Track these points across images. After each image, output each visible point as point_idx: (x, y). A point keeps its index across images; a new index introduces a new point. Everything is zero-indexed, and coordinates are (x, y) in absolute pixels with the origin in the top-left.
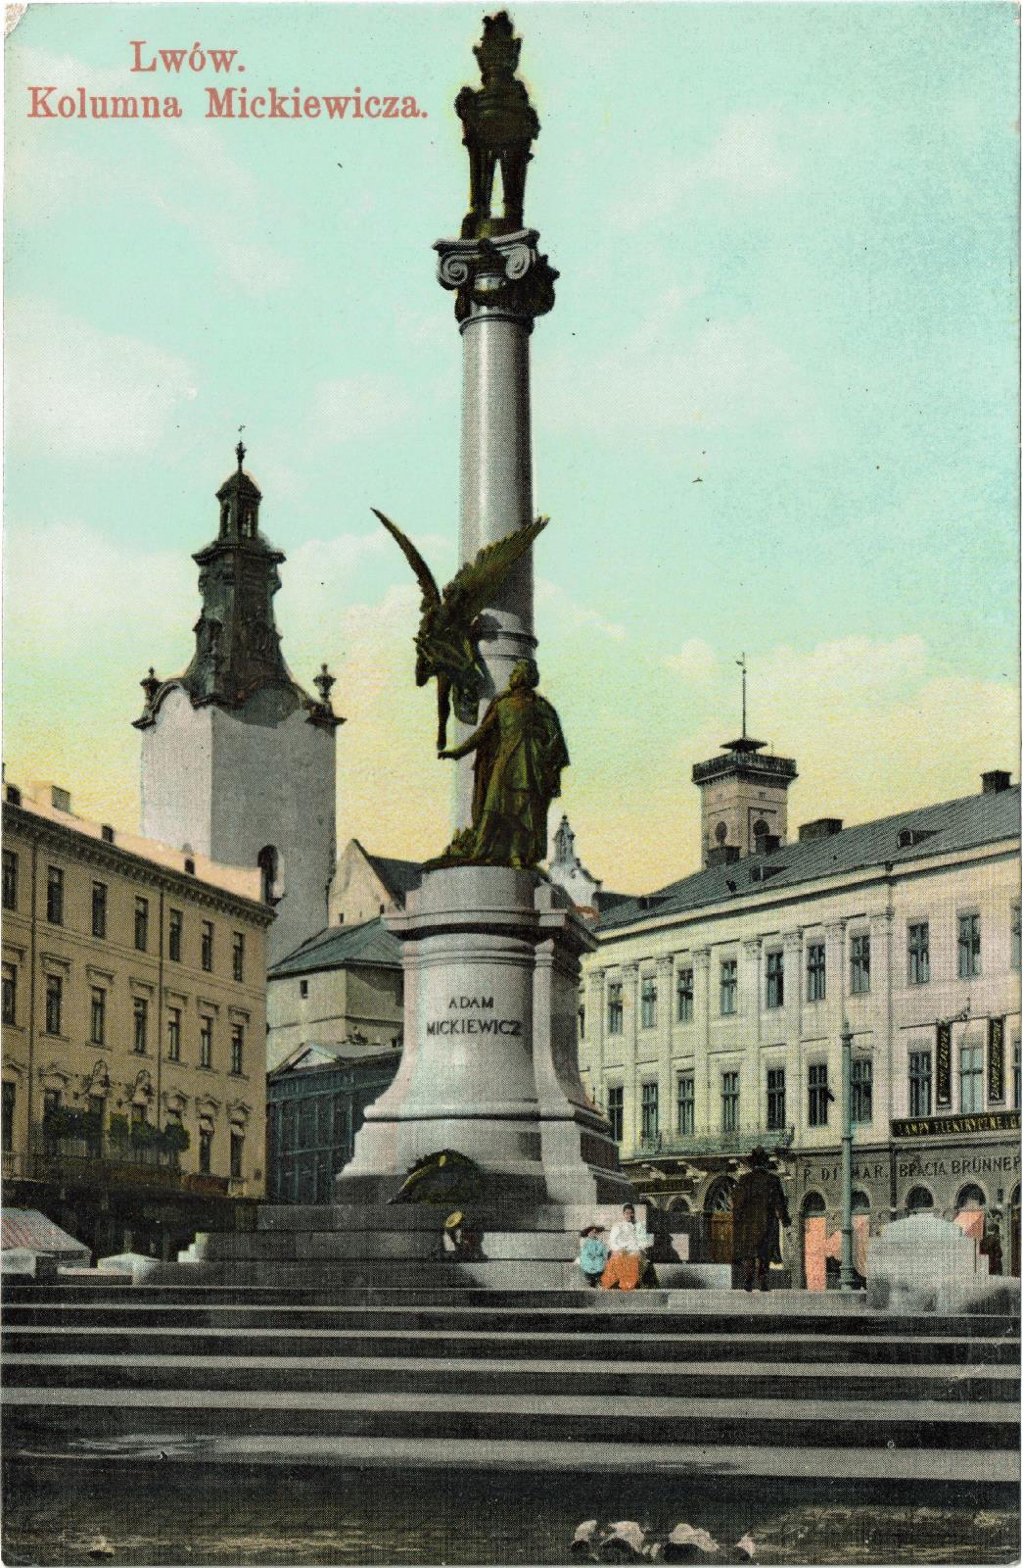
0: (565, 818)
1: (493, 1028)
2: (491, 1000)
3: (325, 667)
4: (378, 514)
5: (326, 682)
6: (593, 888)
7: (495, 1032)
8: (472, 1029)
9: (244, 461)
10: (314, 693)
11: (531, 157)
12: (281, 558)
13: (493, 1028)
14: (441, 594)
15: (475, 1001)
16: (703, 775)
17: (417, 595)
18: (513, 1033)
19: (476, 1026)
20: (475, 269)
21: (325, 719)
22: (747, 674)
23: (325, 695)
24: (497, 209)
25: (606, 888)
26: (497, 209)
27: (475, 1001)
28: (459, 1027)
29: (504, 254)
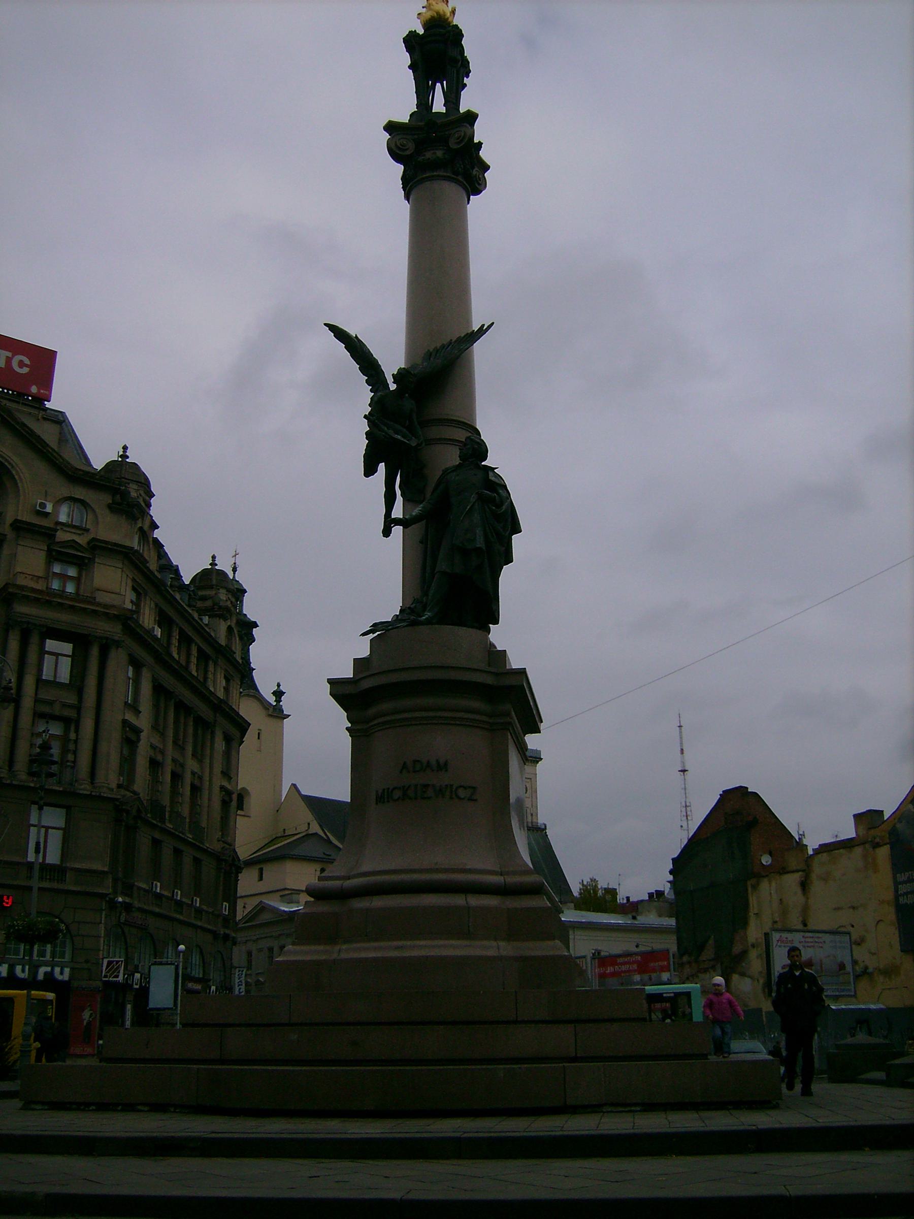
2: (446, 764)
3: (279, 685)
4: (333, 328)
5: (279, 694)
7: (451, 798)
9: (236, 573)
10: (272, 700)
12: (255, 625)
14: (390, 380)
15: (428, 762)
17: (365, 394)
18: (470, 799)
20: (421, 145)
21: (277, 713)
23: (278, 700)
24: (439, 105)
26: (439, 105)
27: (428, 764)
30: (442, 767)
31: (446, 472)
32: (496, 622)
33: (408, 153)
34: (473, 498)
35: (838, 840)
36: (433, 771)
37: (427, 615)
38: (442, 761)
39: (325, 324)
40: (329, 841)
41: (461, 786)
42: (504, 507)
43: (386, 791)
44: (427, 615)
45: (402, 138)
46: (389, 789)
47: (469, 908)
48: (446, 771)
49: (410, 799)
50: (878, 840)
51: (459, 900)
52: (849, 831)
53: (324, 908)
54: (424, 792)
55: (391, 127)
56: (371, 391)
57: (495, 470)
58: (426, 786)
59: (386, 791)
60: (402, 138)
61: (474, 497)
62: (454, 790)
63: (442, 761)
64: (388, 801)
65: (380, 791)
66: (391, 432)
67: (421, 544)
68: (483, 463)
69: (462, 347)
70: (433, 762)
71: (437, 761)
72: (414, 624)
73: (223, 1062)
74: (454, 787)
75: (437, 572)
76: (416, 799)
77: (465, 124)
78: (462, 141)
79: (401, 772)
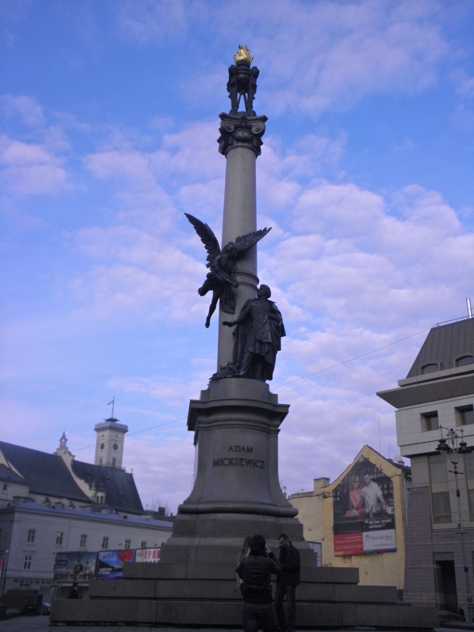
0: (64, 433)
1: (252, 464)
2: (252, 449)
6: (71, 458)
7: (254, 466)
8: (242, 464)
11: (254, 98)
13: (252, 464)
16: (98, 429)
17: (205, 253)
18: (262, 467)
19: (244, 462)
22: (114, 399)
25: (76, 459)
27: (243, 448)
28: (234, 462)
29: (251, 124)
30: (250, 450)
31: (249, 302)
32: (270, 378)
33: (231, 131)
34: (266, 317)
35: (304, 492)
36: (245, 451)
37: (242, 373)
38: (250, 448)
39: (185, 214)
40: (10, 469)
41: (258, 461)
42: (280, 324)
43: (220, 461)
44: (242, 373)
45: (229, 123)
46: (221, 459)
47: (266, 523)
48: (252, 452)
49: (234, 465)
50: (326, 494)
51: (260, 518)
52: (310, 487)
53: (186, 517)
54: (241, 462)
55: (223, 116)
56: (208, 252)
57: (275, 304)
58: (242, 459)
59: (220, 461)
60: (228, 123)
61: (267, 316)
62: (255, 463)
63: (250, 448)
64: (221, 465)
65: (216, 460)
66: (224, 277)
67: (232, 335)
68: (269, 299)
69: (258, 238)
70: (246, 448)
71: (248, 447)
72: (239, 376)
73: (155, 599)
74: (255, 461)
75: (246, 352)
76: (236, 465)
77: (261, 122)
78: (259, 131)
79: (229, 451)
